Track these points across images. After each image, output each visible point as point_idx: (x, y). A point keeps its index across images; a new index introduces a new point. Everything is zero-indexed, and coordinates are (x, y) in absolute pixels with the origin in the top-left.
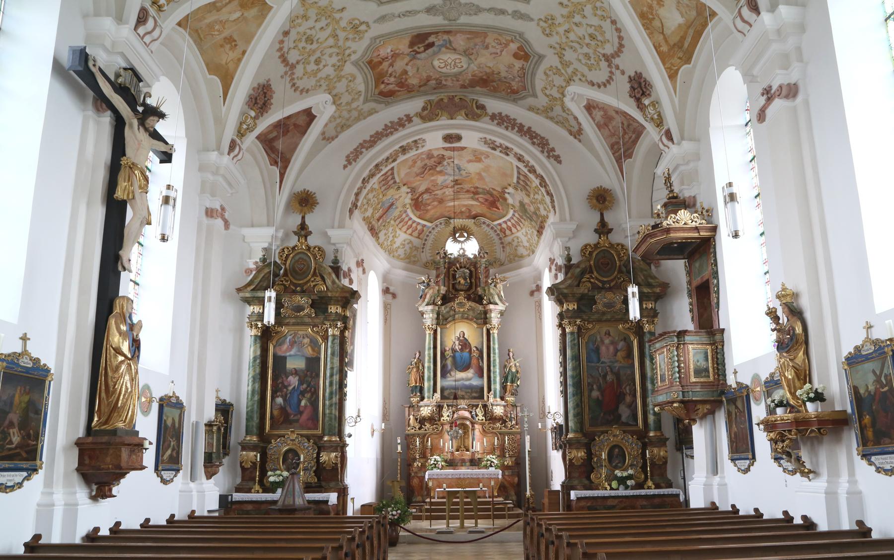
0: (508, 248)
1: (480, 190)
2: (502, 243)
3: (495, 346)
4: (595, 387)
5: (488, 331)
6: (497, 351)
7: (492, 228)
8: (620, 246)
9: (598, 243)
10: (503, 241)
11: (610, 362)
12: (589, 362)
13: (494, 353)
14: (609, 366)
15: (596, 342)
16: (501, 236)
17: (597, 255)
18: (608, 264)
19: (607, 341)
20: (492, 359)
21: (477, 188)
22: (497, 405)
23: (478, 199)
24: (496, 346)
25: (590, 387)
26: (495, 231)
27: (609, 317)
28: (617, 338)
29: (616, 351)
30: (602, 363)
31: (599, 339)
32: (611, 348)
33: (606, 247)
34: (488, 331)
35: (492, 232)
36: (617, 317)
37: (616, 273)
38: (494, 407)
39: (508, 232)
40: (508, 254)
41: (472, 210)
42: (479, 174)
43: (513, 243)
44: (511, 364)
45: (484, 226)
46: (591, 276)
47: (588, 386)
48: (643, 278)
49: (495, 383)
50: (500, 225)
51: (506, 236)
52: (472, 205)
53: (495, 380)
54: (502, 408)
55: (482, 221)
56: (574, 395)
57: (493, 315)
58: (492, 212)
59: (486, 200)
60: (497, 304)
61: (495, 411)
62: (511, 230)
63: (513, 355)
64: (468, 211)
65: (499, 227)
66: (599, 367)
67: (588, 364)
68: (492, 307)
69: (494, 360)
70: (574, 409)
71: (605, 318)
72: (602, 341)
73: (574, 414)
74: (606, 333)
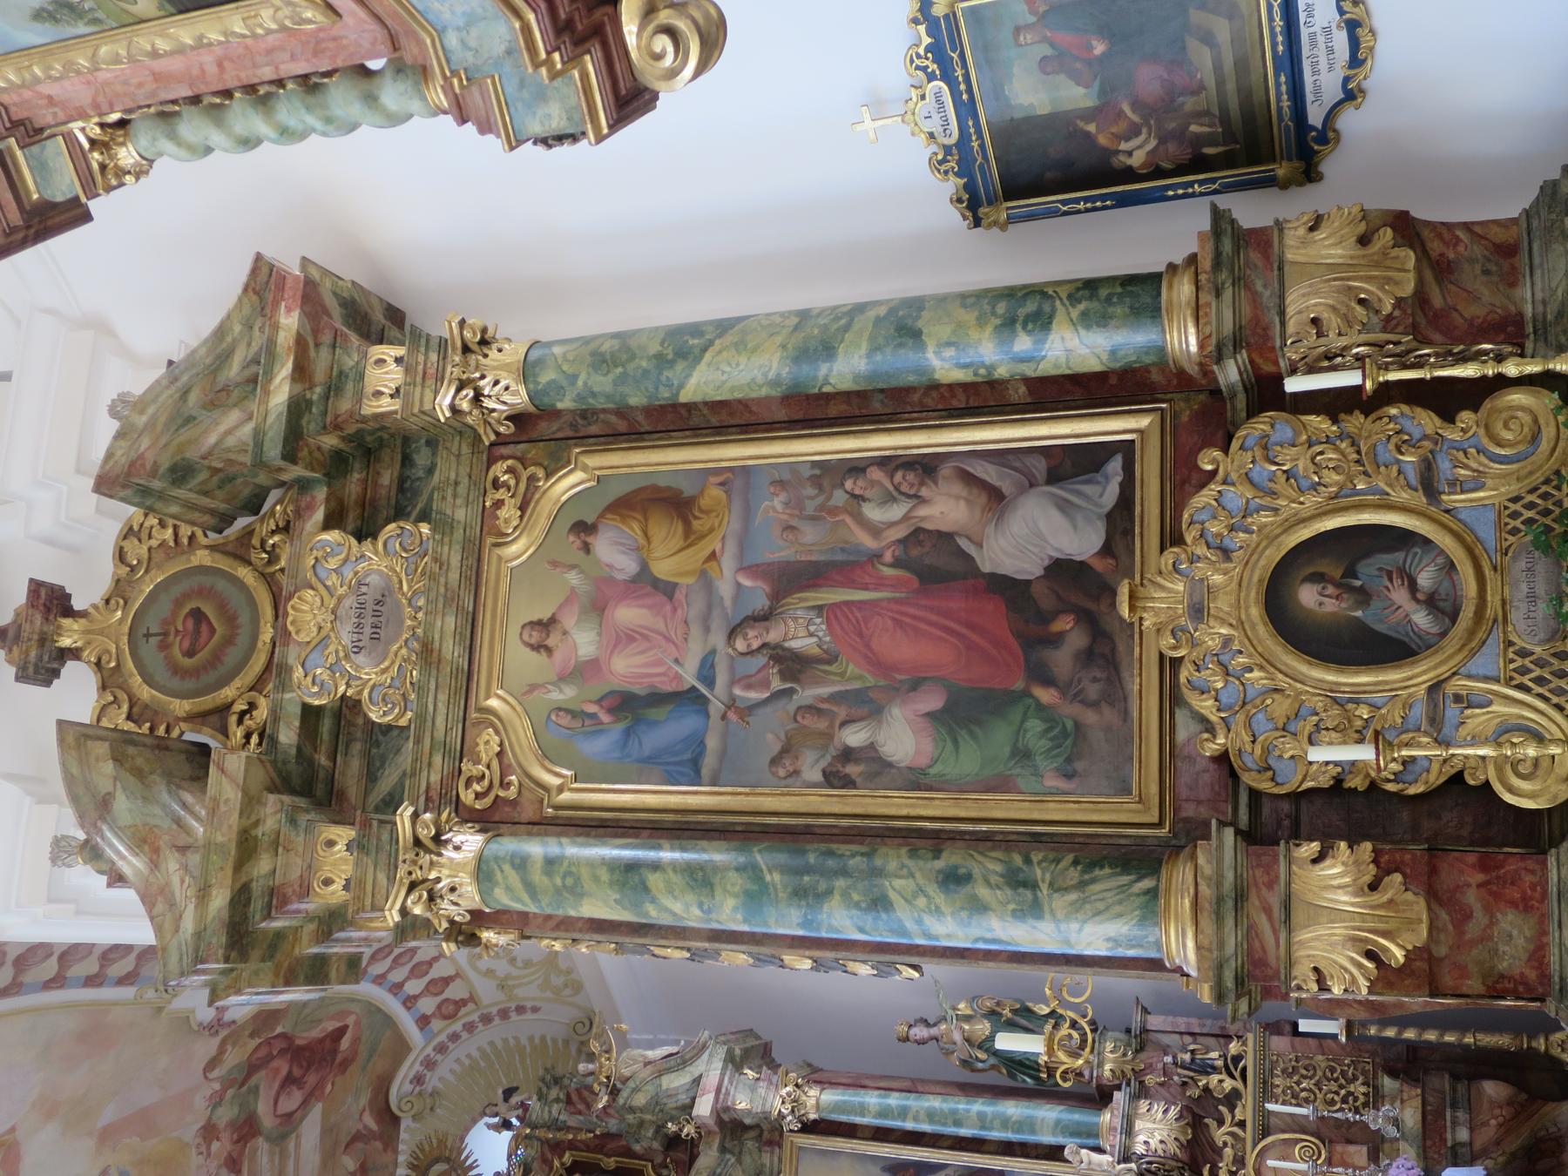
0: (520, 992)
1: (226, 1114)
2: (504, 1014)
3: (871, 1105)
4: (854, 737)
5: (809, 1128)
6: (894, 1100)
7: (441, 1049)
8: (127, 545)
9: (98, 664)
10: (494, 1010)
11: (707, 630)
12: (696, 763)
13: (903, 1113)
14: (732, 634)
15: (574, 714)
16: (475, 1017)
17: (148, 680)
18: (198, 615)
19: (584, 641)
20: (926, 1127)
21: (209, 1132)
22: (1129, 1131)
23: (289, 1115)
24: (872, 1099)
25: (852, 770)
26: (455, 1037)
27: (450, 622)
28: (573, 578)
29: (647, 584)
30: (710, 682)
31: (566, 694)
32: (628, 614)
33: (121, 621)
34: (809, 1128)
35: (459, 1051)
36: (454, 576)
37: (243, 573)
38: (1140, 1149)
39: (455, 991)
40: (548, 994)
41: (353, 1126)
42: (107, 1136)
43: (501, 973)
44: (957, 1037)
45: (433, 1081)
46: (242, 714)
47: (848, 783)
48: (234, 416)
49: (1029, 1124)
50: (423, 1021)
51: (472, 999)
52: (328, 1130)
53: (1020, 1126)
54: (1143, 1105)
55: (408, 1087)
56: (879, 903)
57: (742, 1103)
58: (363, 1050)
59: (289, 1081)
60: (697, 1081)
61: (1154, 1143)
62: (446, 981)
63: (926, 1023)
64: (360, 1145)
65: (436, 1024)
66: (732, 704)
67: (706, 772)
68: (704, 1108)
69: (931, 1116)
70: (979, 907)
71: (451, 650)
72: (586, 670)
73: (1020, 914)
74: (537, 648)
